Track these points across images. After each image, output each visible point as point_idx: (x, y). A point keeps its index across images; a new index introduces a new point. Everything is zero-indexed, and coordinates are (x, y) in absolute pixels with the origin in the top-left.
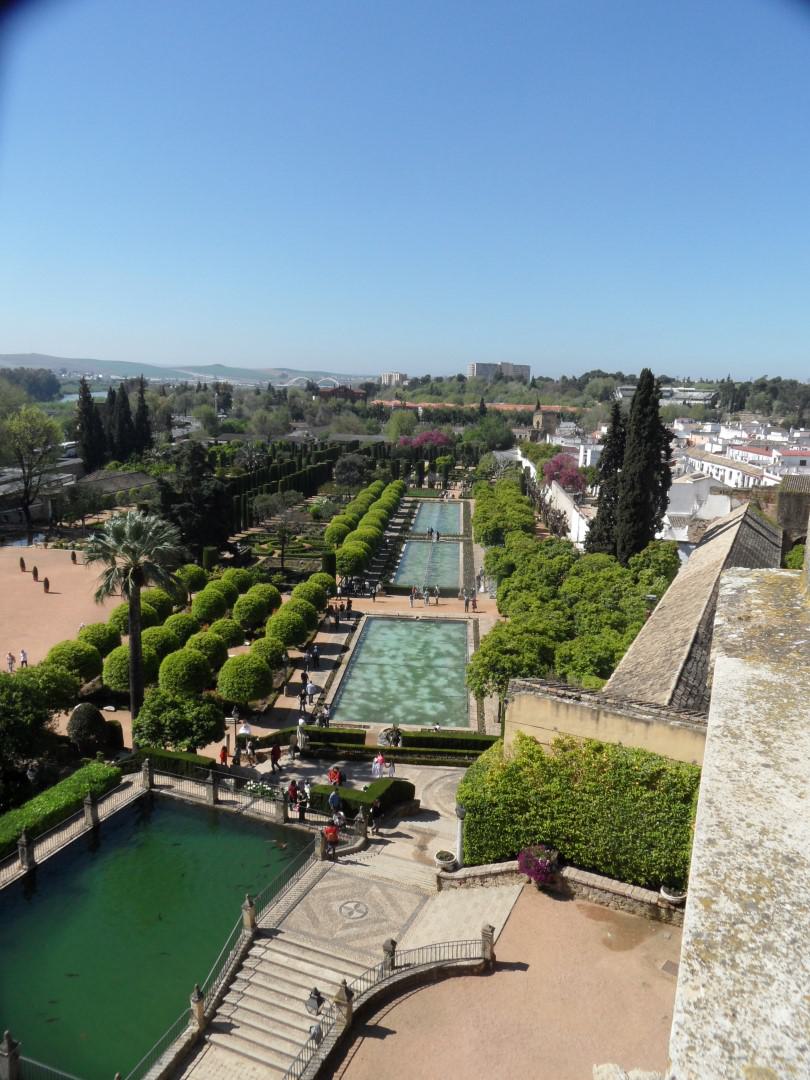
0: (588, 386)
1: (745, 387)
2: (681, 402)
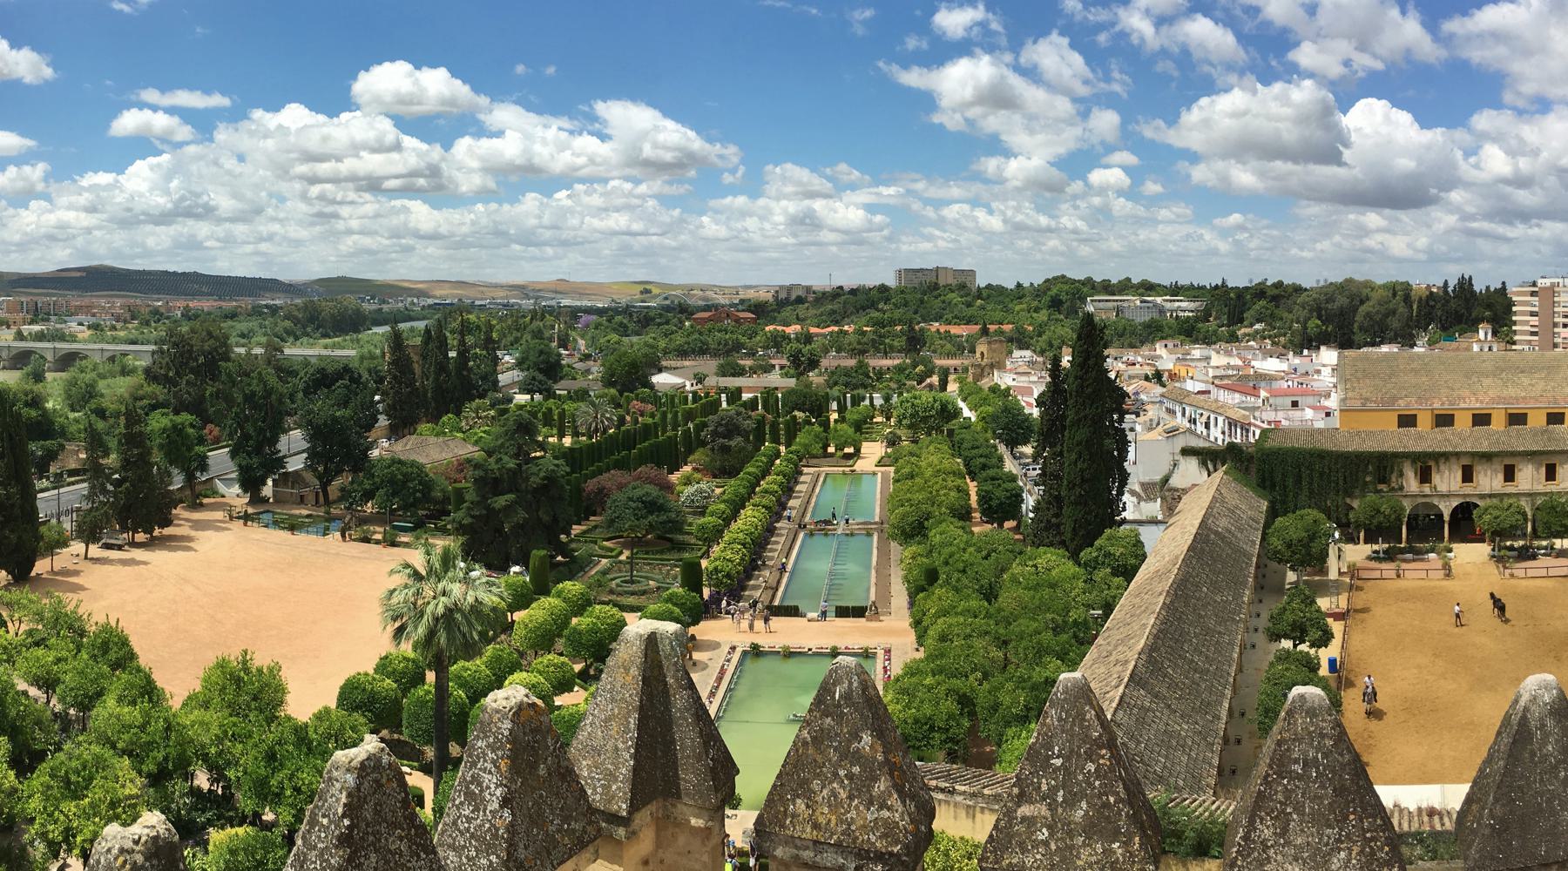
1: (1241, 293)
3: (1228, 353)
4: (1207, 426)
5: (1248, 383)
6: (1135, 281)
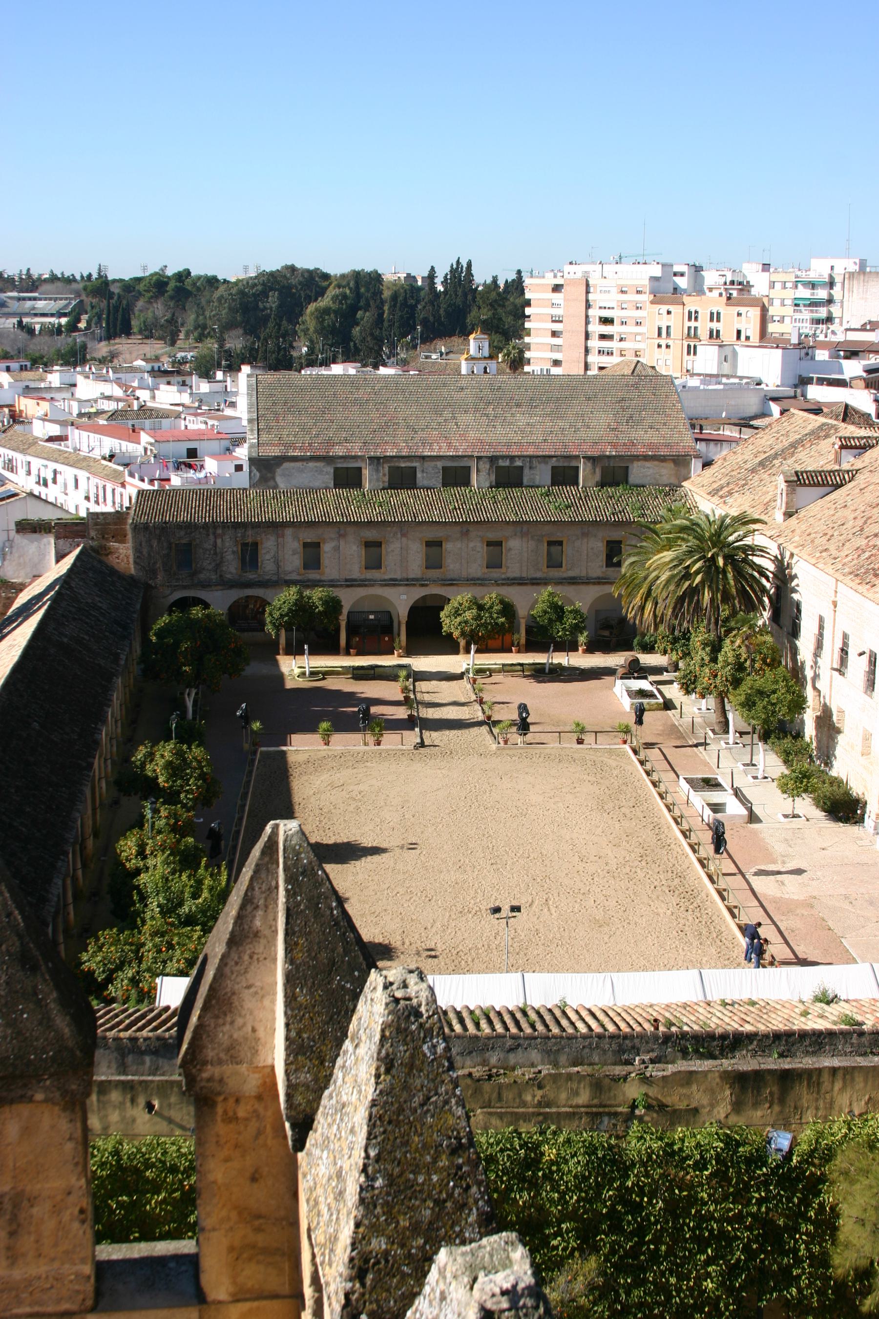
1: (131, 287)
2: (15, 320)
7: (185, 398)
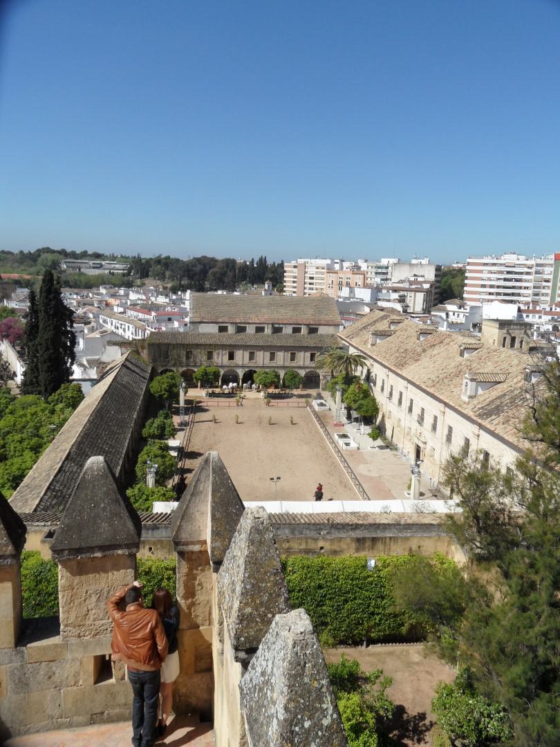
0: (40, 260)
1: (149, 261)
3: (138, 292)
4: (124, 330)
5: (147, 308)
6: (90, 252)
7: (167, 300)
